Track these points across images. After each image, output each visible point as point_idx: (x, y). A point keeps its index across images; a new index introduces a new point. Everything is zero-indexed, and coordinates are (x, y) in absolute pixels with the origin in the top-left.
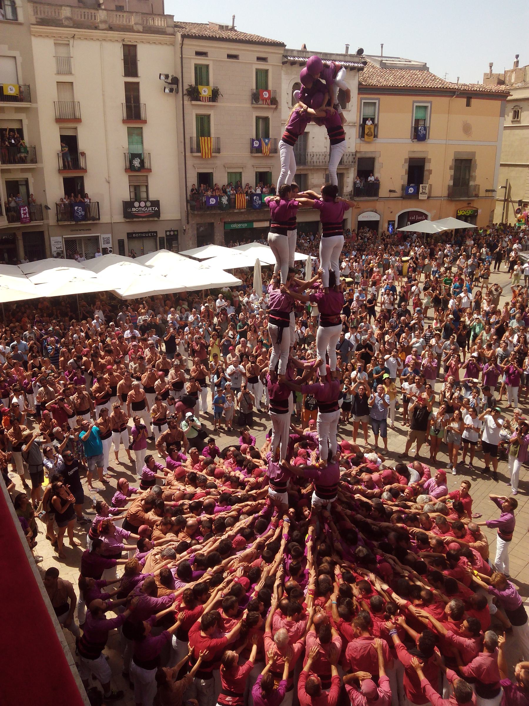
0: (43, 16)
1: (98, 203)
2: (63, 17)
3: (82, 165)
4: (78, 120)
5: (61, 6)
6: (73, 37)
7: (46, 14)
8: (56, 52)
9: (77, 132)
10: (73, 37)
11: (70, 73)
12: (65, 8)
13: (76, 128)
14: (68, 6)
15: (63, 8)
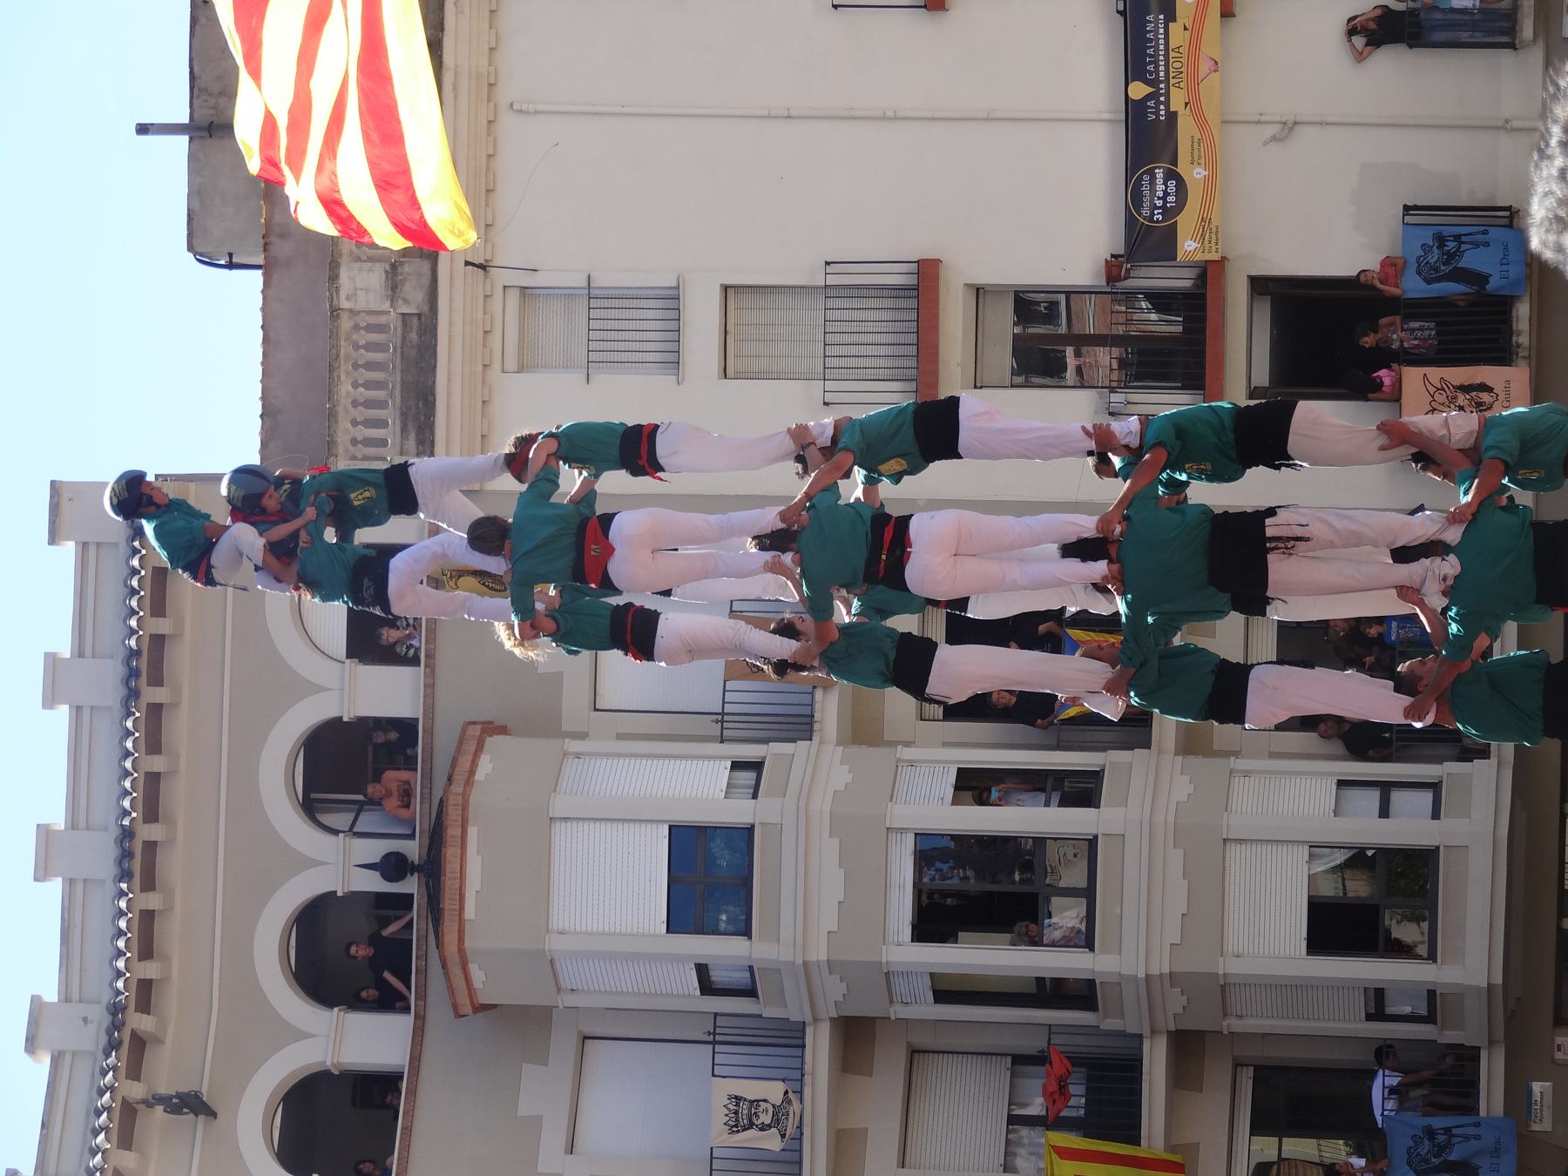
0: (390, 414)
1: (1407, 208)
2: (386, 306)
3: (1187, 284)
4: (927, 274)
5: (335, 312)
6: (483, 267)
7: (380, 394)
8: (567, 365)
9: (998, 291)
10: (483, 267)
11: (672, 299)
12: (343, 294)
13: (979, 292)
14: (334, 278)
15: (345, 304)
